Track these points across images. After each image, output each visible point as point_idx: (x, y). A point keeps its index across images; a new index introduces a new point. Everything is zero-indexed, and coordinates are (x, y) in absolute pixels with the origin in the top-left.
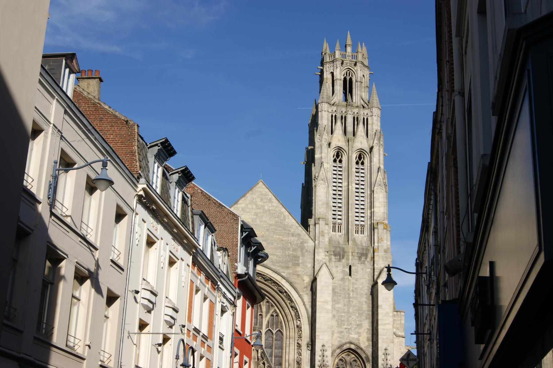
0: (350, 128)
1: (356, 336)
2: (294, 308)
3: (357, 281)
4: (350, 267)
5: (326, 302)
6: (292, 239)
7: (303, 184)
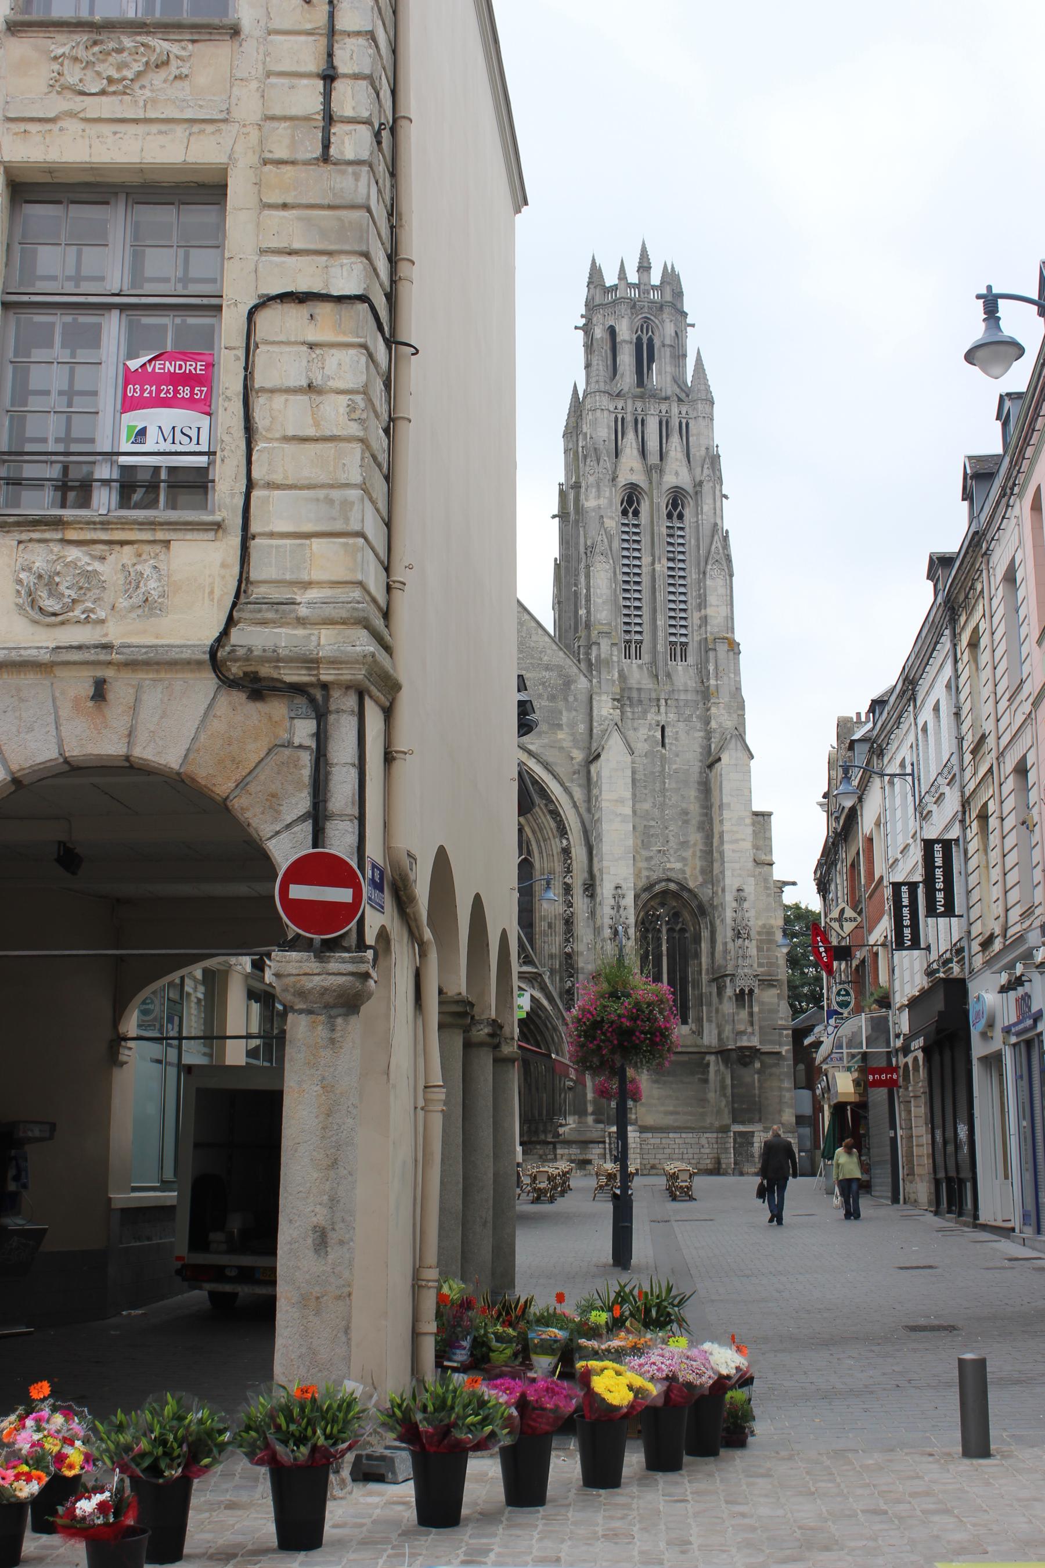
0: (652, 444)
1: (678, 866)
2: (555, 814)
3: (677, 756)
4: (663, 728)
5: (621, 801)
6: (547, 674)
7: (556, 559)
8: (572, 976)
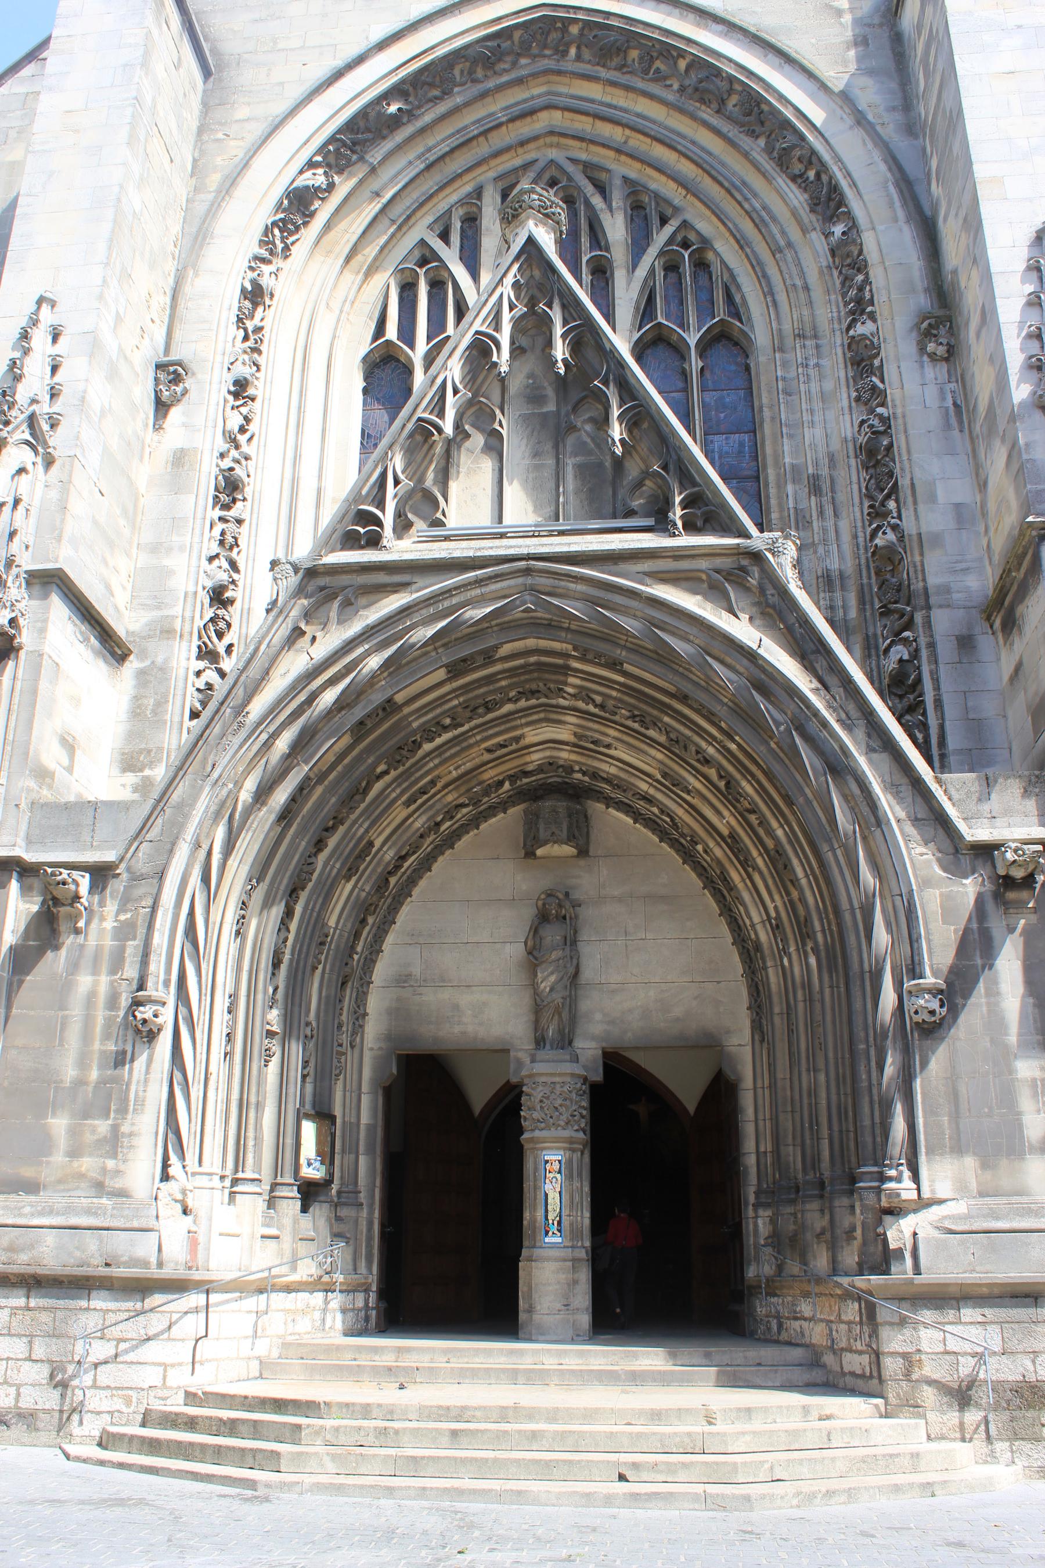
8: (909, 625)
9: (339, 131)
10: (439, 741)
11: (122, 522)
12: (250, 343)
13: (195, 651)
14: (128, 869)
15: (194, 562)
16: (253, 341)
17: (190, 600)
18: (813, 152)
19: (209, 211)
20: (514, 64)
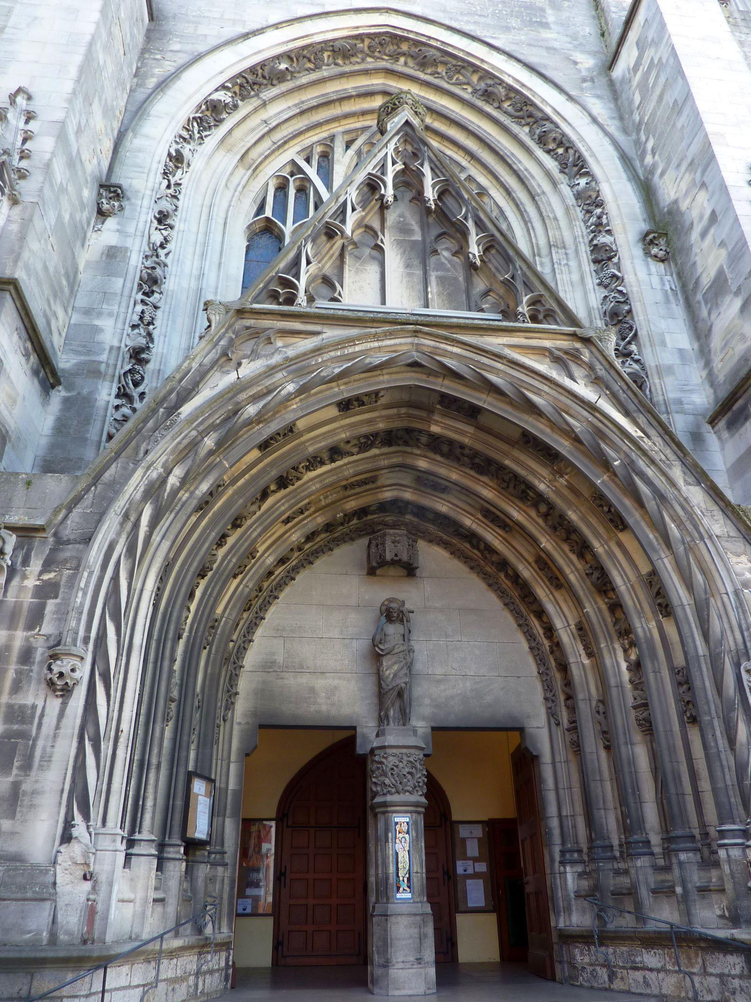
9: (244, 71)
10: (320, 471)
11: (64, 283)
12: (171, 191)
13: (114, 391)
14: (55, 535)
15: (120, 325)
16: (174, 191)
17: (114, 352)
18: (564, 135)
19: (148, 98)
20: (363, 60)
